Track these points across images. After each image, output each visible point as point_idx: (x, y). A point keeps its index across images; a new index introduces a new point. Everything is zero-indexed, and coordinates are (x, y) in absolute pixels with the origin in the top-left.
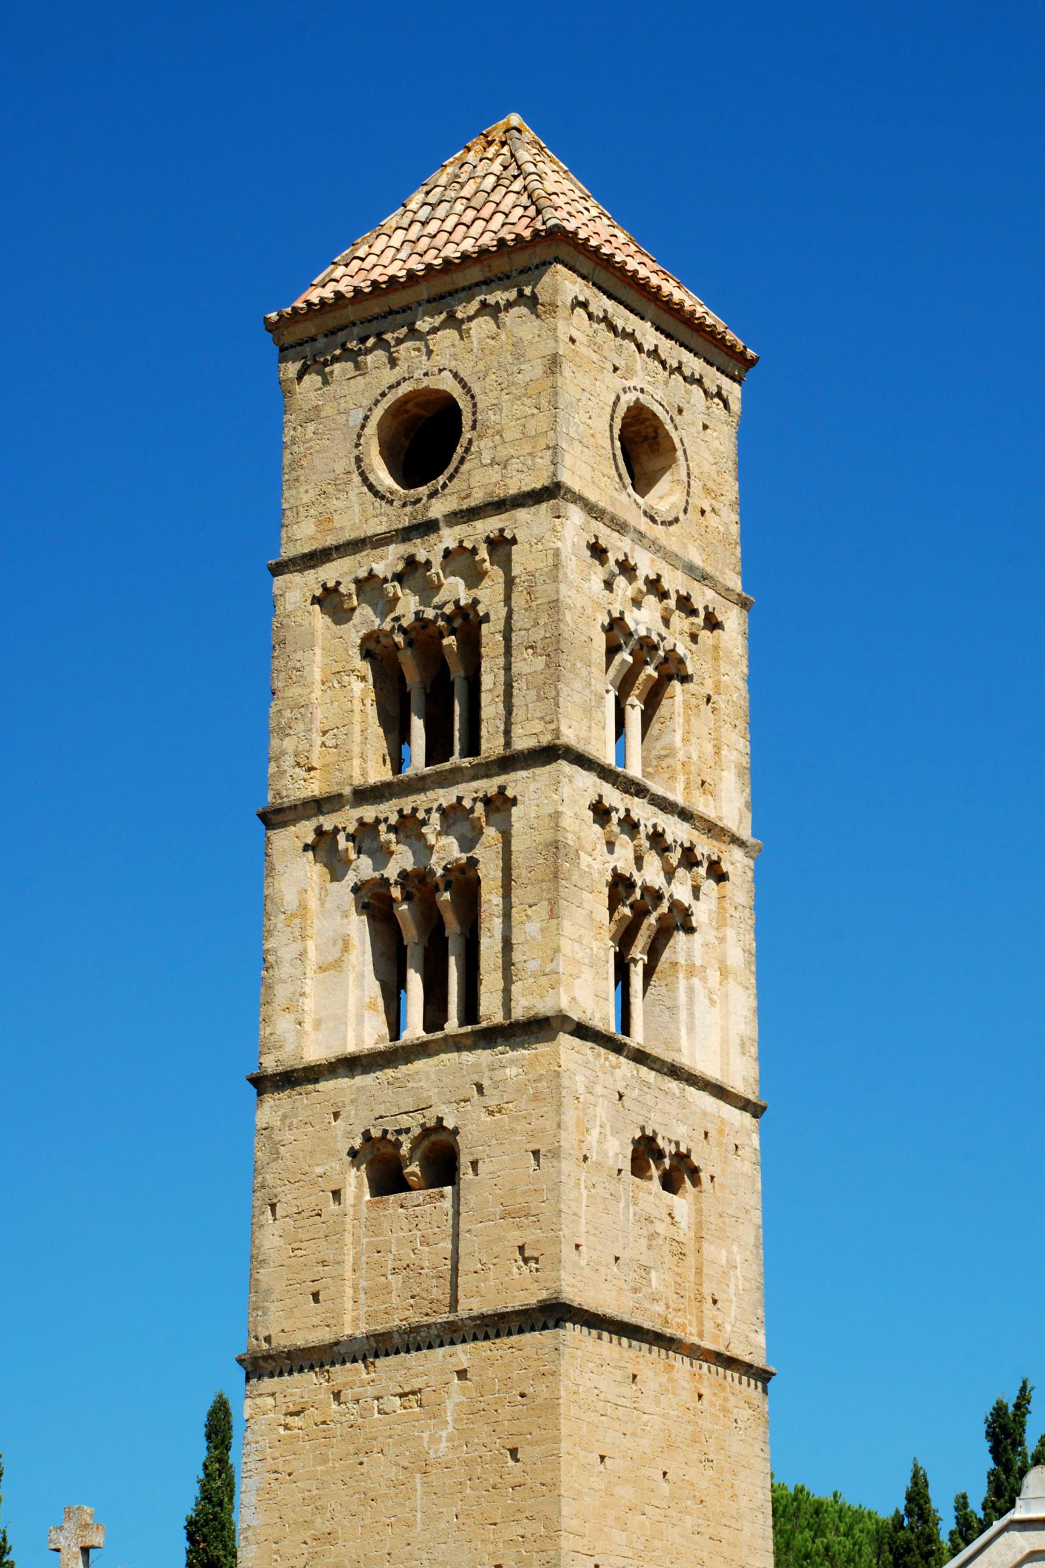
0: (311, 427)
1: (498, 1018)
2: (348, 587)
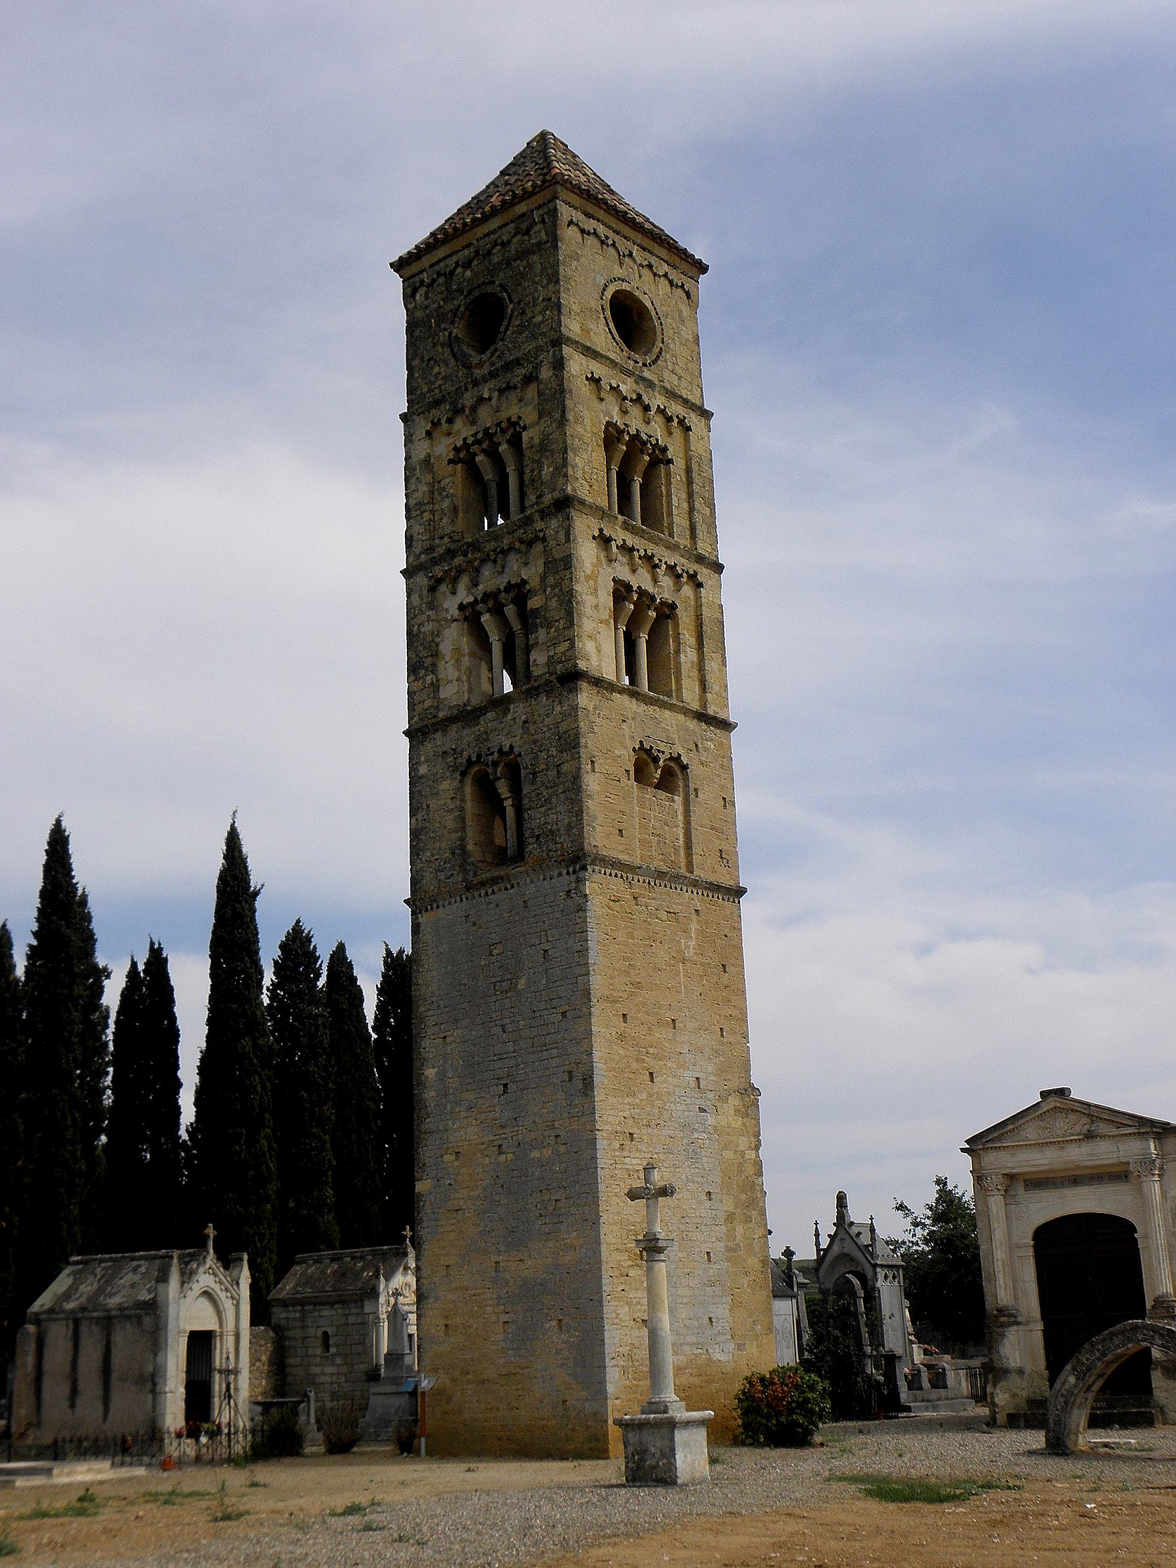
0: (574, 264)
1: (695, 706)
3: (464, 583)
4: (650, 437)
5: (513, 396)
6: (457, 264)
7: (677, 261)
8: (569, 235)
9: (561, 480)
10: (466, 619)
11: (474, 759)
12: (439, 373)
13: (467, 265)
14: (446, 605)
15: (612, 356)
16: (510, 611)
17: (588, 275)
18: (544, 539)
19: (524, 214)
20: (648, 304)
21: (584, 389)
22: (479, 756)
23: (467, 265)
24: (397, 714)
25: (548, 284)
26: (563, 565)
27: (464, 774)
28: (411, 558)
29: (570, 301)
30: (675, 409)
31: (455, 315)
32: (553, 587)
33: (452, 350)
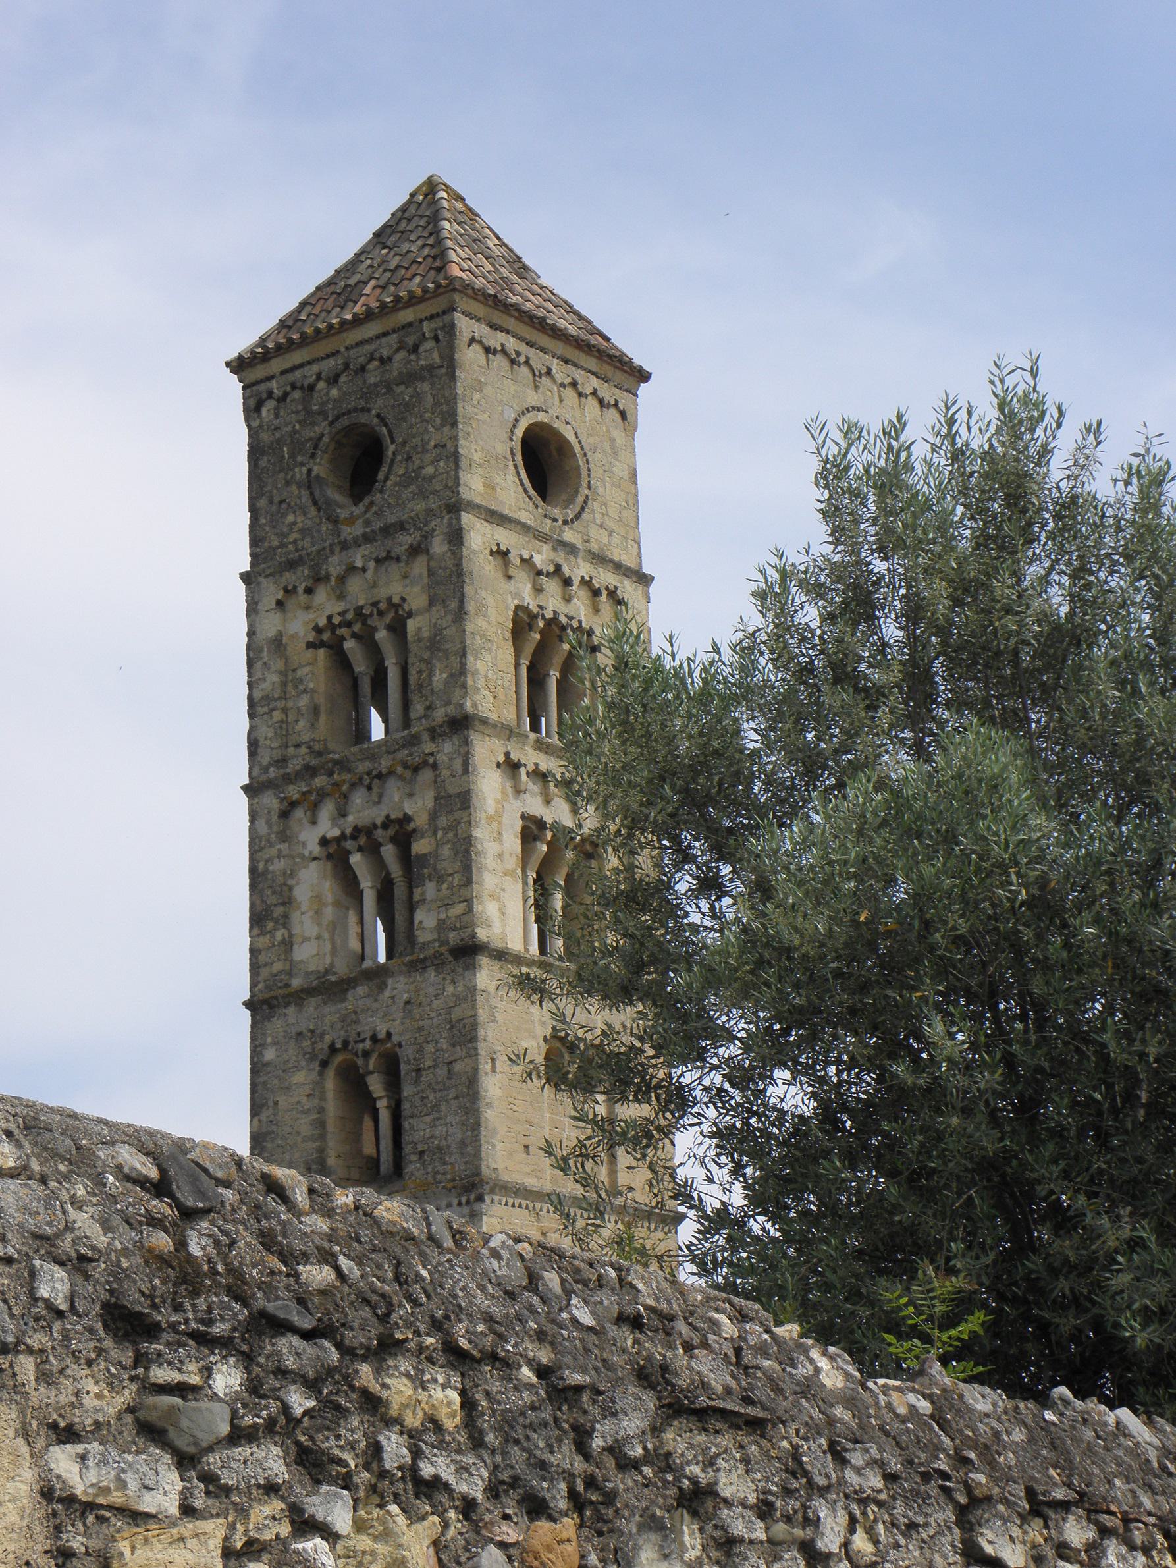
0: (476, 396)
2: (514, 558)
3: (327, 810)
4: (571, 618)
5: (395, 569)
6: (319, 377)
7: (608, 370)
8: (470, 358)
9: (458, 692)
10: (329, 857)
11: (339, 1045)
12: (294, 523)
13: (334, 380)
14: (303, 836)
15: (525, 517)
16: (389, 852)
17: (494, 402)
18: (434, 766)
19: (410, 324)
20: (571, 437)
21: (488, 568)
22: (346, 1043)
23: (334, 380)
24: (238, 982)
25: (443, 426)
26: (458, 803)
27: (324, 1064)
28: (256, 772)
29: (471, 449)
30: (605, 578)
31: (316, 447)
32: (446, 831)
33: (312, 494)
